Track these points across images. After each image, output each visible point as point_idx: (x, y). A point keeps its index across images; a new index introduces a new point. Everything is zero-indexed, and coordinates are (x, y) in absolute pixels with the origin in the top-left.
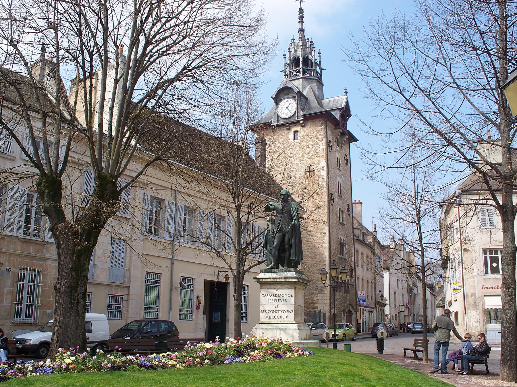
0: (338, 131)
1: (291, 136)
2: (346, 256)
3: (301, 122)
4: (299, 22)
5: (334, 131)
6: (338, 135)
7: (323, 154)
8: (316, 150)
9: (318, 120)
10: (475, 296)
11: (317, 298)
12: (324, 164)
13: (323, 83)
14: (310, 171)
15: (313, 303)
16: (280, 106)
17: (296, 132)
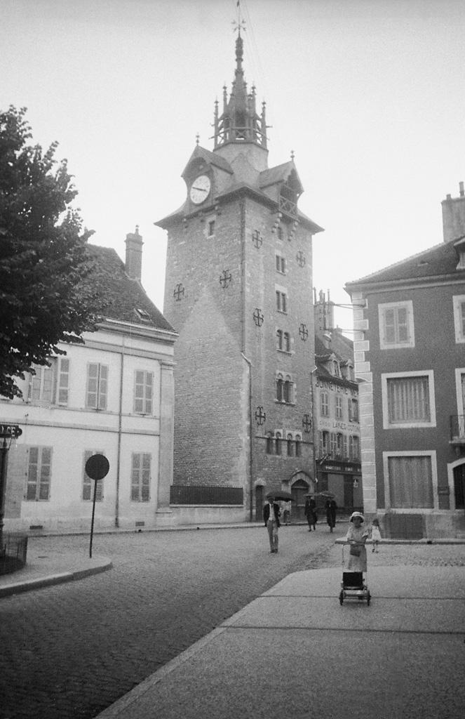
0: (276, 215)
1: (206, 231)
2: (294, 401)
3: (216, 208)
4: (236, 60)
13: (268, 148)
17: (212, 223)
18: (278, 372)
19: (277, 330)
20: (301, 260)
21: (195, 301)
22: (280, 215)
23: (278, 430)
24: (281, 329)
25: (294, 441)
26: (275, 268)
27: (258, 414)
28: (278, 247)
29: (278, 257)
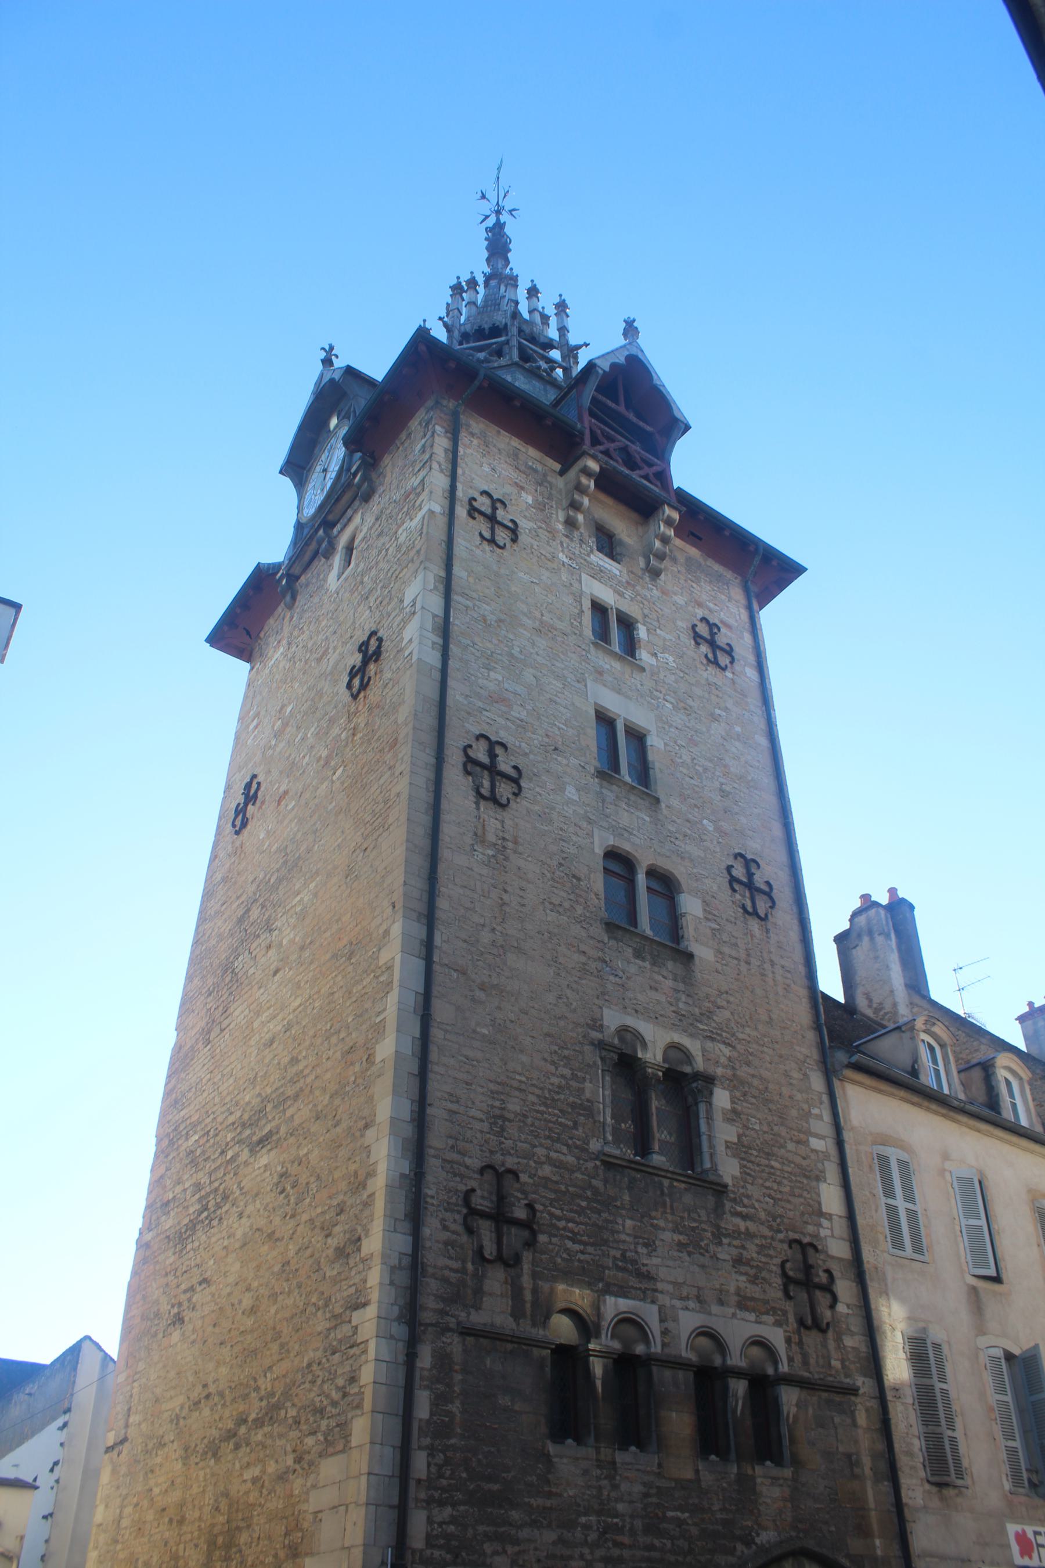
0: (572, 473)
4: (488, 260)
5: (560, 482)
9: (414, 424)
18: (613, 1019)
19: (599, 851)
20: (712, 644)
23: (624, 1304)
24: (627, 847)
25: (738, 1373)
26: (588, 632)
27: (482, 1201)
28: (598, 574)
29: (599, 609)
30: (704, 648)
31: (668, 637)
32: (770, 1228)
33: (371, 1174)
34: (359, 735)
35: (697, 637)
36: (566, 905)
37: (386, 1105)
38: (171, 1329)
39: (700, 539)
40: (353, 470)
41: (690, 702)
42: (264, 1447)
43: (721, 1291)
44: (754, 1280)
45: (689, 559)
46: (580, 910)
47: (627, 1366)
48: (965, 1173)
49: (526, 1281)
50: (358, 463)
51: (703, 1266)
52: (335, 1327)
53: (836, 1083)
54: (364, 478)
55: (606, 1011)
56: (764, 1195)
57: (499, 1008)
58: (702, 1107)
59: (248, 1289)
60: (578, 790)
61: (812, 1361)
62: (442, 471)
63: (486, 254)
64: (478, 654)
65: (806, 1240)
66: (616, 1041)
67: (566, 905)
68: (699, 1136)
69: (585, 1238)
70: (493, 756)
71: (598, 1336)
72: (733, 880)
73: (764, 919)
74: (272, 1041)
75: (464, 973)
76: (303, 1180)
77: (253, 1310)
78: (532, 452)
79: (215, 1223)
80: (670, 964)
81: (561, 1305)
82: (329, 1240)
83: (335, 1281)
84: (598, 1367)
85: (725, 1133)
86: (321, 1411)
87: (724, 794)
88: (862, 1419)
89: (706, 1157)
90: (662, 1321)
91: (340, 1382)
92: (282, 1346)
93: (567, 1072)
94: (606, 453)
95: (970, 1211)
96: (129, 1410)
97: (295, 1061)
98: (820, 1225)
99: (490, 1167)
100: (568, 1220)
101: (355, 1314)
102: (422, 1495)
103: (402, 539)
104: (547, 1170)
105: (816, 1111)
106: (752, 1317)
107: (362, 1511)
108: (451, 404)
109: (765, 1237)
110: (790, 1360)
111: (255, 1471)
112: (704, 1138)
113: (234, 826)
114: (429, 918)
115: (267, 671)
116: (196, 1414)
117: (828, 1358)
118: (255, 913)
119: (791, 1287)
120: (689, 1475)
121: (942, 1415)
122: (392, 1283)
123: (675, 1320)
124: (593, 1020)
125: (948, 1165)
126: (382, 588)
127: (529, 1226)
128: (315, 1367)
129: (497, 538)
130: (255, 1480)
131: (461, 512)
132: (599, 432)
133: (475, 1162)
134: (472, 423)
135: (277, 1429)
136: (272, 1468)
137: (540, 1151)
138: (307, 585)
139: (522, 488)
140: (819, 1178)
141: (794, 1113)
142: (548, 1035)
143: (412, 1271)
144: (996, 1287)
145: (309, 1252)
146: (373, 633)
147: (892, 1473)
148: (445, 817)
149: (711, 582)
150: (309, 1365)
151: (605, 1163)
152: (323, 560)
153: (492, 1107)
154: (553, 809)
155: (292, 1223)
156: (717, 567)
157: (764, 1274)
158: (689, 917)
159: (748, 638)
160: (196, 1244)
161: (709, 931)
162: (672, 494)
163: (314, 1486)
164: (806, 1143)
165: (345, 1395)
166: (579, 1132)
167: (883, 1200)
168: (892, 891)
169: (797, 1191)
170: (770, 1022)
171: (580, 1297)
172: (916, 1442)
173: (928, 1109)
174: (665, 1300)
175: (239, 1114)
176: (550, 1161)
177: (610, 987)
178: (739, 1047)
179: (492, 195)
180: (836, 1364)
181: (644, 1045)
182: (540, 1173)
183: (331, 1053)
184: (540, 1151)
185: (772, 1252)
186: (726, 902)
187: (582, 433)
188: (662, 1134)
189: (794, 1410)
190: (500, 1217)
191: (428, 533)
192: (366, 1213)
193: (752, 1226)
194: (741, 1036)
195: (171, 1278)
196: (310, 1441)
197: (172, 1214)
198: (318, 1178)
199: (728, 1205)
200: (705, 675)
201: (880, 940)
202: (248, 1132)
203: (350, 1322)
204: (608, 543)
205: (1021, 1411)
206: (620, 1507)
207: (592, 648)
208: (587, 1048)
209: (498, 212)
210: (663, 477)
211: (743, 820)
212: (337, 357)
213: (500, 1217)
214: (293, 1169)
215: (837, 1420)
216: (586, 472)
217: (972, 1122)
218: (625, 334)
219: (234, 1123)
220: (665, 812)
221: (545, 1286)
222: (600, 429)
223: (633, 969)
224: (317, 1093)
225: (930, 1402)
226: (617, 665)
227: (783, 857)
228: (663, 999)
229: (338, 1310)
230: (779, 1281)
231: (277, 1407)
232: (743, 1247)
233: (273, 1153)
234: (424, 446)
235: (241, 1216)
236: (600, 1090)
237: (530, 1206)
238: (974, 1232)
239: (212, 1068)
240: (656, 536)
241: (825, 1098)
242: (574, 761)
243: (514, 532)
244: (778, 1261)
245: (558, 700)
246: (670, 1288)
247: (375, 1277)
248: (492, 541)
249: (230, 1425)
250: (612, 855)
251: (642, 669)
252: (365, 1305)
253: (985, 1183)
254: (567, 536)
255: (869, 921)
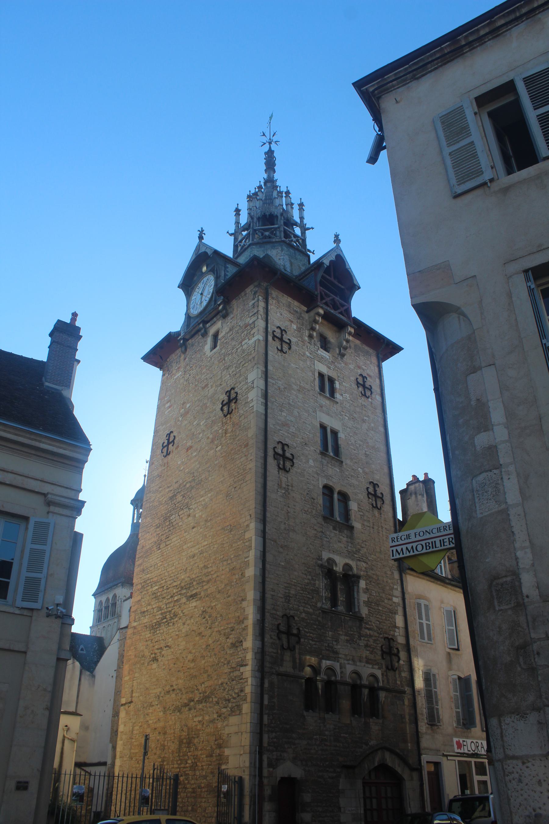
0: (312, 313)
4: (266, 170)
5: (306, 316)
6: (316, 322)
7: (253, 355)
8: (243, 351)
9: (248, 290)
10: (515, 588)
11: (227, 731)
12: (254, 375)
14: (231, 400)
15: (220, 746)
16: (193, 298)
18: (326, 555)
19: (321, 487)
20: (364, 386)
21: (187, 450)
22: (321, 311)
23: (328, 663)
24: (331, 484)
25: (365, 686)
26: (317, 389)
27: (283, 628)
28: (321, 360)
29: (321, 375)
30: (361, 389)
31: (347, 385)
32: (378, 633)
33: (246, 618)
34: (228, 435)
35: (358, 383)
36: (310, 510)
37: (251, 594)
38: (152, 662)
39: (361, 336)
40: (219, 303)
41: (355, 415)
42: (203, 710)
43: (360, 657)
44: (372, 653)
45: (356, 346)
46: (314, 512)
47: (329, 684)
48: (449, 608)
49: (297, 656)
50: (221, 301)
51: (354, 648)
52: (233, 672)
53: (404, 575)
54: (224, 308)
55: (323, 553)
56: (376, 621)
57: (287, 554)
58: (356, 588)
59: (190, 652)
60: (313, 461)
61: (390, 682)
62: (262, 319)
63: (264, 167)
64: (277, 405)
65: (390, 637)
66: (326, 564)
67: (310, 510)
68: (354, 599)
69: (316, 639)
70: (284, 451)
71: (320, 674)
72: (369, 493)
73: (380, 509)
74: (194, 556)
75: (276, 542)
76: (214, 615)
77: (193, 661)
78: (296, 303)
79: (171, 624)
80: (345, 531)
81: (308, 664)
82: (228, 640)
83: (231, 655)
84: (320, 685)
85: (363, 597)
86: (229, 700)
87: (367, 455)
88: (406, 702)
89: (356, 607)
90: (341, 668)
91: (236, 691)
92: (209, 676)
93: (310, 577)
94: (326, 304)
95: (450, 624)
96: (132, 691)
97: (206, 567)
98: (395, 631)
99: (286, 615)
100: (311, 633)
101: (242, 668)
102: (266, 729)
103: (245, 347)
104: (303, 615)
105: (395, 587)
106: (371, 666)
107: (249, 734)
108: (265, 284)
109: (376, 637)
110: (383, 681)
111: (200, 718)
112: (356, 600)
113: (162, 452)
114: (263, 520)
115: (172, 381)
116: (168, 696)
117: (396, 681)
118: (179, 498)
119: (384, 655)
120: (348, 722)
121: (434, 700)
122: (255, 658)
123: (345, 668)
124: (319, 556)
125: (442, 605)
126: (235, 367)
127: (298, 636)
128: (224, 685)
129: (283, 349)
130: (199, 722)
131: (270, 338)
132: (323, 293)
133: (280, 613)
134: (273, 292)
135: (208, 705)
136: (207, 718)
137: (301, 608)
138: (193, 345)
139: (292, 322)
140: (396, 613)
141: (388, 588)
142: (304, 563)
143: (261, 655)
144: (457, 652)
145: (219, 643)
146: (233, 389)
147: (415, 721)
148: (268, 479)
149: (364, 355)
150: (222, 684)
151: (323, 611)
152: (200, 337)
153: (286, 592)
154: (304, 470)
155: (210, 631)
156: (367, 348)
157: (375, 650)
158: (353, 511)
159: (378, 380)
160: (162, 631)
161: (359, 516)
162: (352, 320)
163: (227, 725)
164: (391, 600)
165: (238, 696)
166: (314, 600)
167: (418, 621)
168: (426, 474)
169: (388, 619)
170: (380, 552)
171: (313, 660)
172: (425, 710)
173: (437, 583)
174: (342, 661)
175: (179, 583)
176: (305, 612)
177: (325, 543)
178: (369, 563)
179: (267, 134)
180: (398, 682)
181: (336, 565)
182: (301, 616)
183: (224, 568)
184: (301, 608)
185: (378, 642)
186: (366, 502)
187: (317, 296)
188: (341, 598)
189: (384, 699)
190: (289, 633)
191: (258, 351)
192: (244, 632)
193: (371, 633)
194: (370, 558)
195: (149, 643)
196: (224, 710)
197: (147, 617)
198: (221, 616)
199: (364, 625)
200: (360, 401)
201: (419, 497)
202: (185, 591)
203: (239, 670)
204: (325, 344)
205: (462, 698)
206: (327, 733)
207: (319, 396)
208: (317, 568)
209: (270, 143)
210: (348, 312)
211: (373, 466)
212: (205, 234)
213: (289, 633)
214: (209, 610)
215: (398, 703)
216: (318, 314)
217: (453, 588)
218: (335, 242)
219: (177, 586)
220: (345, 466)
221: (304, 657)
222: (324, 291)
223: (333, 535)
224: (218, 582)
225: (430, 695)
226: (328, 402)
227: (387, 481)
228: (343, 546)
229: (234, 665)
230: (380, 653)
231: (208, 697)
232: (368, 640)
233: (198, 602)
234: (254, 304)
235: (184, 624)
236: (321, 584)
237: (298, 629)
238: (450, 632)
239: (162, 560)
240: (344, 340)
241: (399, 581)
242: (312, 448)
243: (289, 344)
244: (380, 645)
245: (307, 422)
246: (343, 656)
247: (250, 656)
248: (281, 351)
249: (186, 701)
250: (326, 487)
251: (337, 403)
252: (246, 665)
253: (456, 611)
254: (309, 343)
255: (415, 488)
